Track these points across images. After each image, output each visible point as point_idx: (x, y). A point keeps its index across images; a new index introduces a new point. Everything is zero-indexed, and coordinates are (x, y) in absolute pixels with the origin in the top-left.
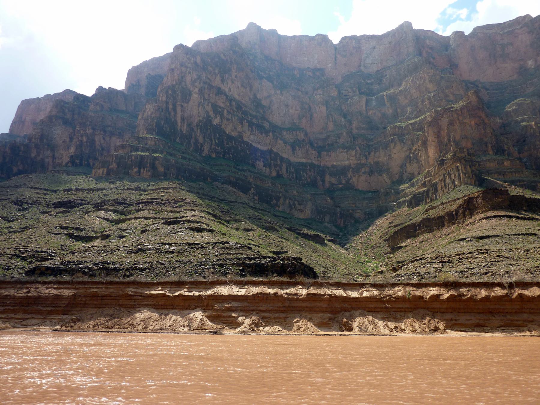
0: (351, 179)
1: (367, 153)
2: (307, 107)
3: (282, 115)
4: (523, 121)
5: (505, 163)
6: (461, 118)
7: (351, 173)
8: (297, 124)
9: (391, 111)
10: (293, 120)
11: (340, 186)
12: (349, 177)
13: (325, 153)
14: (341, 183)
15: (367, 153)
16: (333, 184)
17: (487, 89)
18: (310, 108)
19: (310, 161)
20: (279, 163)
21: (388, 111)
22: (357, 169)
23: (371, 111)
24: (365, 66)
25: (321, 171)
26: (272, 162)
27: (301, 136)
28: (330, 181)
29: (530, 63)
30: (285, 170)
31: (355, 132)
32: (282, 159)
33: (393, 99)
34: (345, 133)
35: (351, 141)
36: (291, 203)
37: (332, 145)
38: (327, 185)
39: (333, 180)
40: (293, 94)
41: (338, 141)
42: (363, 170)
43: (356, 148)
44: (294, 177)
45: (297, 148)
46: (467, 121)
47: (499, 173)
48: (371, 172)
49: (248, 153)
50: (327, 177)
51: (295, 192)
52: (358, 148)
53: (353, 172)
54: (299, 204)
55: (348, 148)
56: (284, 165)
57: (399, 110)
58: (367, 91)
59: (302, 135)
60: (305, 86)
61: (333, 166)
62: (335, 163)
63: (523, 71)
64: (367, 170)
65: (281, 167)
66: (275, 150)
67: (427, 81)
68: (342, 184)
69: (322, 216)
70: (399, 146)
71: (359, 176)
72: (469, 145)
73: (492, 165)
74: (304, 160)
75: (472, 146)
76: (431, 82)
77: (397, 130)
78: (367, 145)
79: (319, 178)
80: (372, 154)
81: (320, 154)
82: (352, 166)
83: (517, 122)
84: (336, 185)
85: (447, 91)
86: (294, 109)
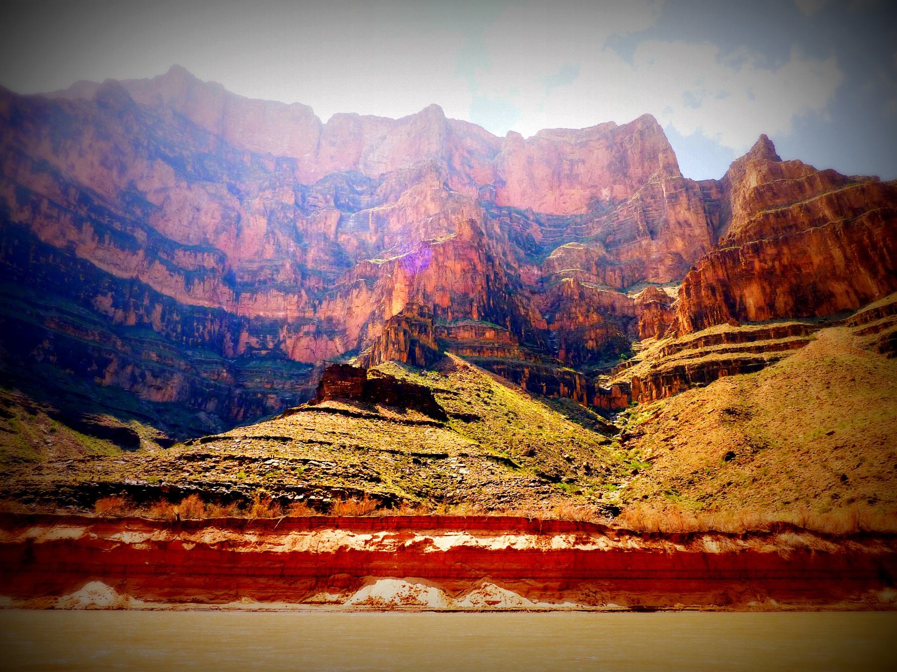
0: (284, 341)
1: (317, 302)
2: (233, 215)
3: (185, 223)
4: (566, 276)
5: (487, 334)
6: (441, 259)
7: (285, 331)
8: (211, 242)
9: (374, 238)
10: (205, 234)
11: (264, 352)
12: (281, 338)
13: (248, 295)
14: (265, 348)
15: (317, 302)
16: (251, 348)
17: (541, 224)
18: (239, 218)
19: (216, 306)
20: (146, 302)
21: (371, 238)
22: (296, 327)
23: (344, 236)
24: (365, 165)
25: (236, 325)
26: (132, 300)
27: (210, 262)
28: (247, 343)
29: (605, 194)
30: (159, 317)
31: (310, 265)
32: (156, 297)
33: (380, 220)
34: (288, 266)
35: (296, 280)
36: (137, 372)
37: (265, 282)
38: (242, 349)
39: (254, 341)
40: (213, 191)
41: (275, 276)
42: (306, 329)
43: (300, 292)
44: (179, 330)
45: (196, 281)
46: (449, 263)
47: (474, 349)
48: (318, 334)
49: (82, 279)
50: (245, 336)
51: (154, 356)
52: (303, 292)
53: (289, 331)
54: (155, 376)
55: (285, 290)
56: (159, 308)
57: (386, 239)
58: (351, 204)
59: (212, 261)
60: (248, 182)
61: (258, 318)
62: (261, 314)
63: (594, 203)
64: (313, 329)
65: (148, 311)
66: (144, 279)
67: (428, 198)
68: (267, 349)
69: (200, 400)
70: (364, 295)
71: (298, 339)
72: (446, 302)
73: (466, 335)
74: (206, 304)
75: (450, 304)
76: (433, 199)
77: (368, 269)
78: (324, 288)
79: (228, 335)
80: (325, 304)
81: (238, 295)
82: (290, 321)
83: (558, 277)
84: (257, 349)
85: (453, 217)
86: (210, 215)
